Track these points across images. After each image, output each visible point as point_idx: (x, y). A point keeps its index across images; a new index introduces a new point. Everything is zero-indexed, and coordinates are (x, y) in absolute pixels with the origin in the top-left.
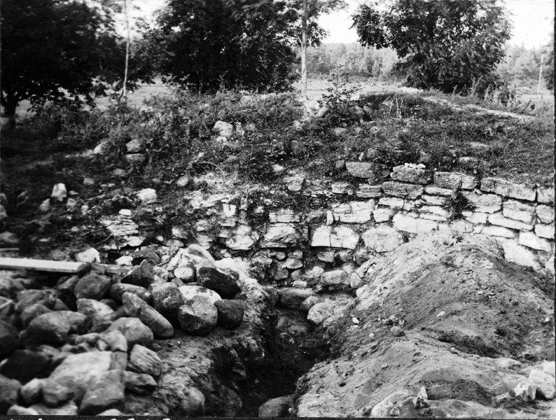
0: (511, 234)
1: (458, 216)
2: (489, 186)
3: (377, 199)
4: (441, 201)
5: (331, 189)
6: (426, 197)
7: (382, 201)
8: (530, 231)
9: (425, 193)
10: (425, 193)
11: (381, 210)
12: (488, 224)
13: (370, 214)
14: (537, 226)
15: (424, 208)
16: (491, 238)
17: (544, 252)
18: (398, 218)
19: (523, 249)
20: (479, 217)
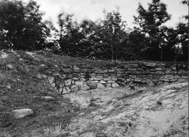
0: (98, 81)
1: (88, 80)
2: (94, 71)
3: (72, 78)
4: (84, 76)
5: (63, 77)
6: (81, 76)
7: (73, 78)
8: (102, 80)
9: (81, 75)
10: (81, 75)
11: (73, 81)
12: (94, 80)
13: (71, 83)
14: (104, 79)
15: (81, 79)
16: (95, 83)
17: (105, 84)
18: (76, 83)
19: (101, 84)
20: (92, 79)
